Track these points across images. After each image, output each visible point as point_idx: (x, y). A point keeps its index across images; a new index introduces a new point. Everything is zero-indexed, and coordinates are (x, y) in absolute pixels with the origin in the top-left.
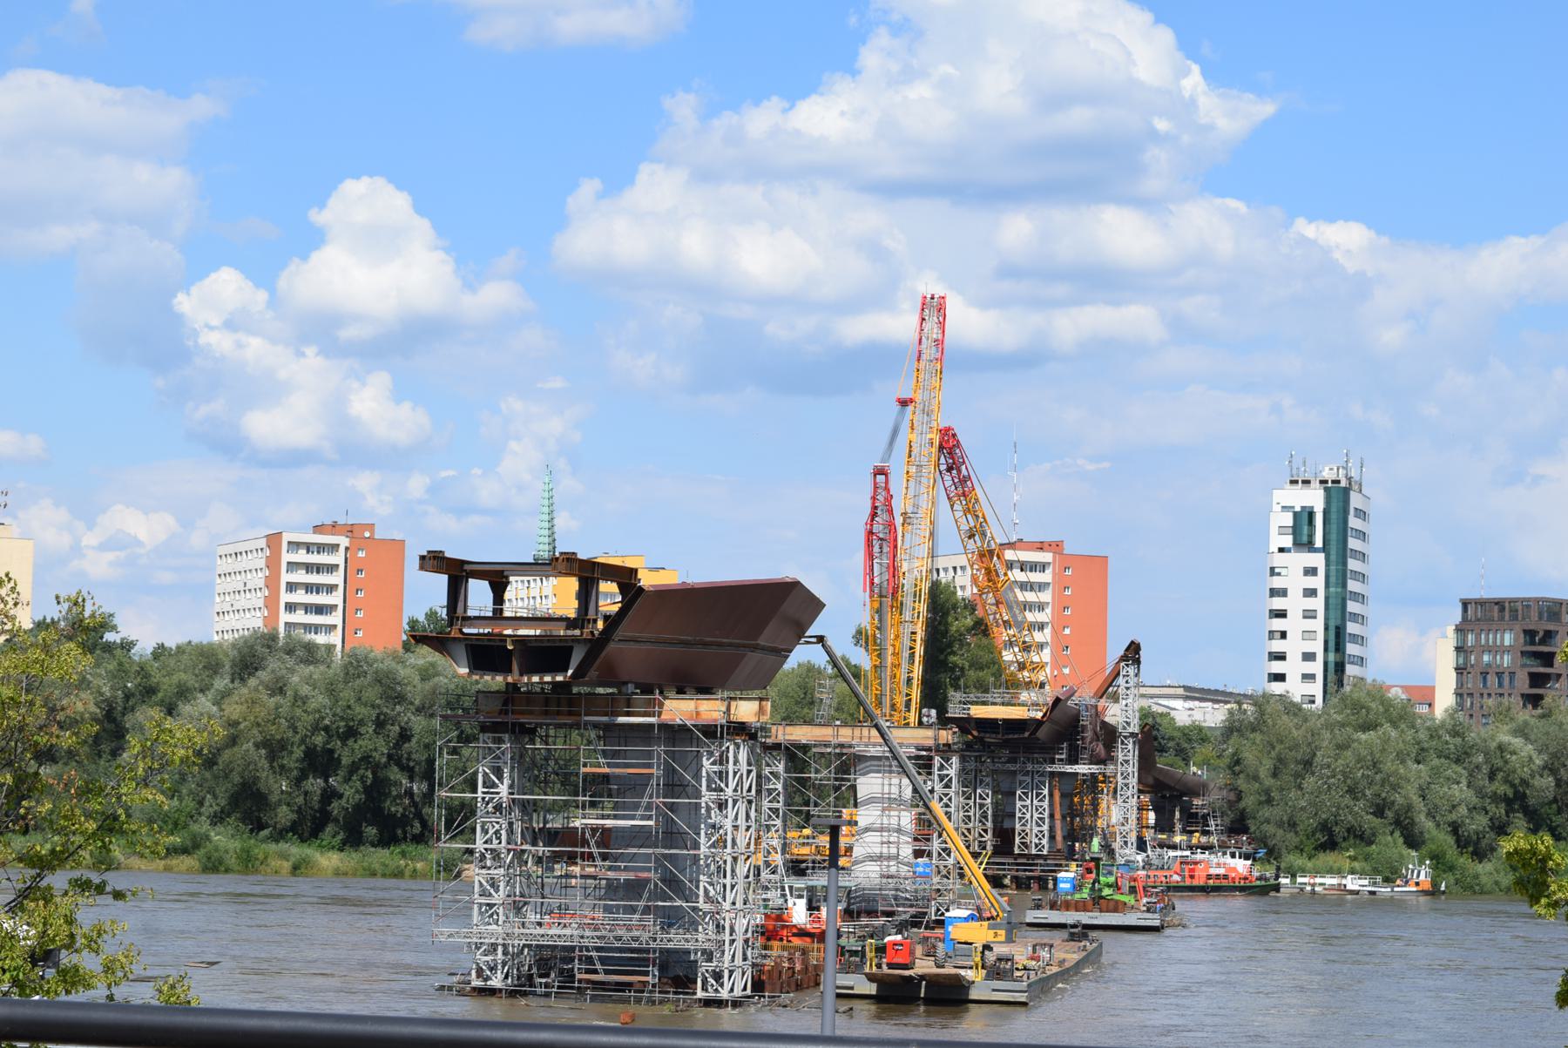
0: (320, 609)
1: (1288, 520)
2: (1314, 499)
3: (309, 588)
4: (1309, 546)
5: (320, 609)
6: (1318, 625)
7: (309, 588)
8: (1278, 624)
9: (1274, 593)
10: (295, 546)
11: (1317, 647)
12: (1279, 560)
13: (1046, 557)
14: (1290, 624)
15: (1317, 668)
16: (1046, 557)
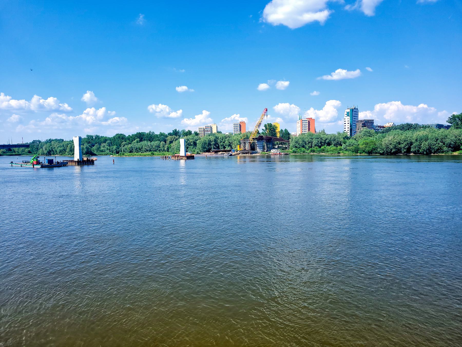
0: (237, 130)
1: (346, 113)
2: (349, 111)
3: (236, 128)
4: (349, 116)
5: (237, 130)
6: (349, 124)
7: (236, 128)
8: (345, 125)
9: (345, 121)
10: (234, 124)
11: (349, 127)
12: (345, 118)
13: (307, 120)
14: (347, 124)
15: (349, 129)
16: (307, 120)
